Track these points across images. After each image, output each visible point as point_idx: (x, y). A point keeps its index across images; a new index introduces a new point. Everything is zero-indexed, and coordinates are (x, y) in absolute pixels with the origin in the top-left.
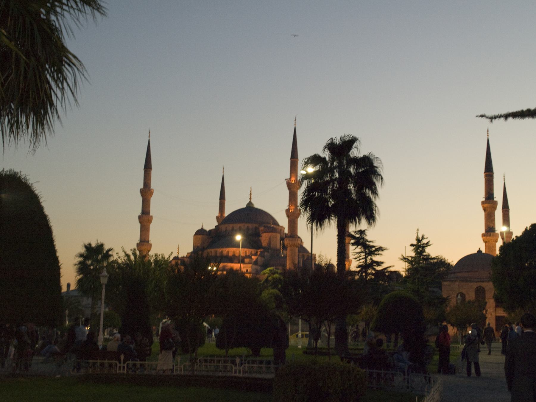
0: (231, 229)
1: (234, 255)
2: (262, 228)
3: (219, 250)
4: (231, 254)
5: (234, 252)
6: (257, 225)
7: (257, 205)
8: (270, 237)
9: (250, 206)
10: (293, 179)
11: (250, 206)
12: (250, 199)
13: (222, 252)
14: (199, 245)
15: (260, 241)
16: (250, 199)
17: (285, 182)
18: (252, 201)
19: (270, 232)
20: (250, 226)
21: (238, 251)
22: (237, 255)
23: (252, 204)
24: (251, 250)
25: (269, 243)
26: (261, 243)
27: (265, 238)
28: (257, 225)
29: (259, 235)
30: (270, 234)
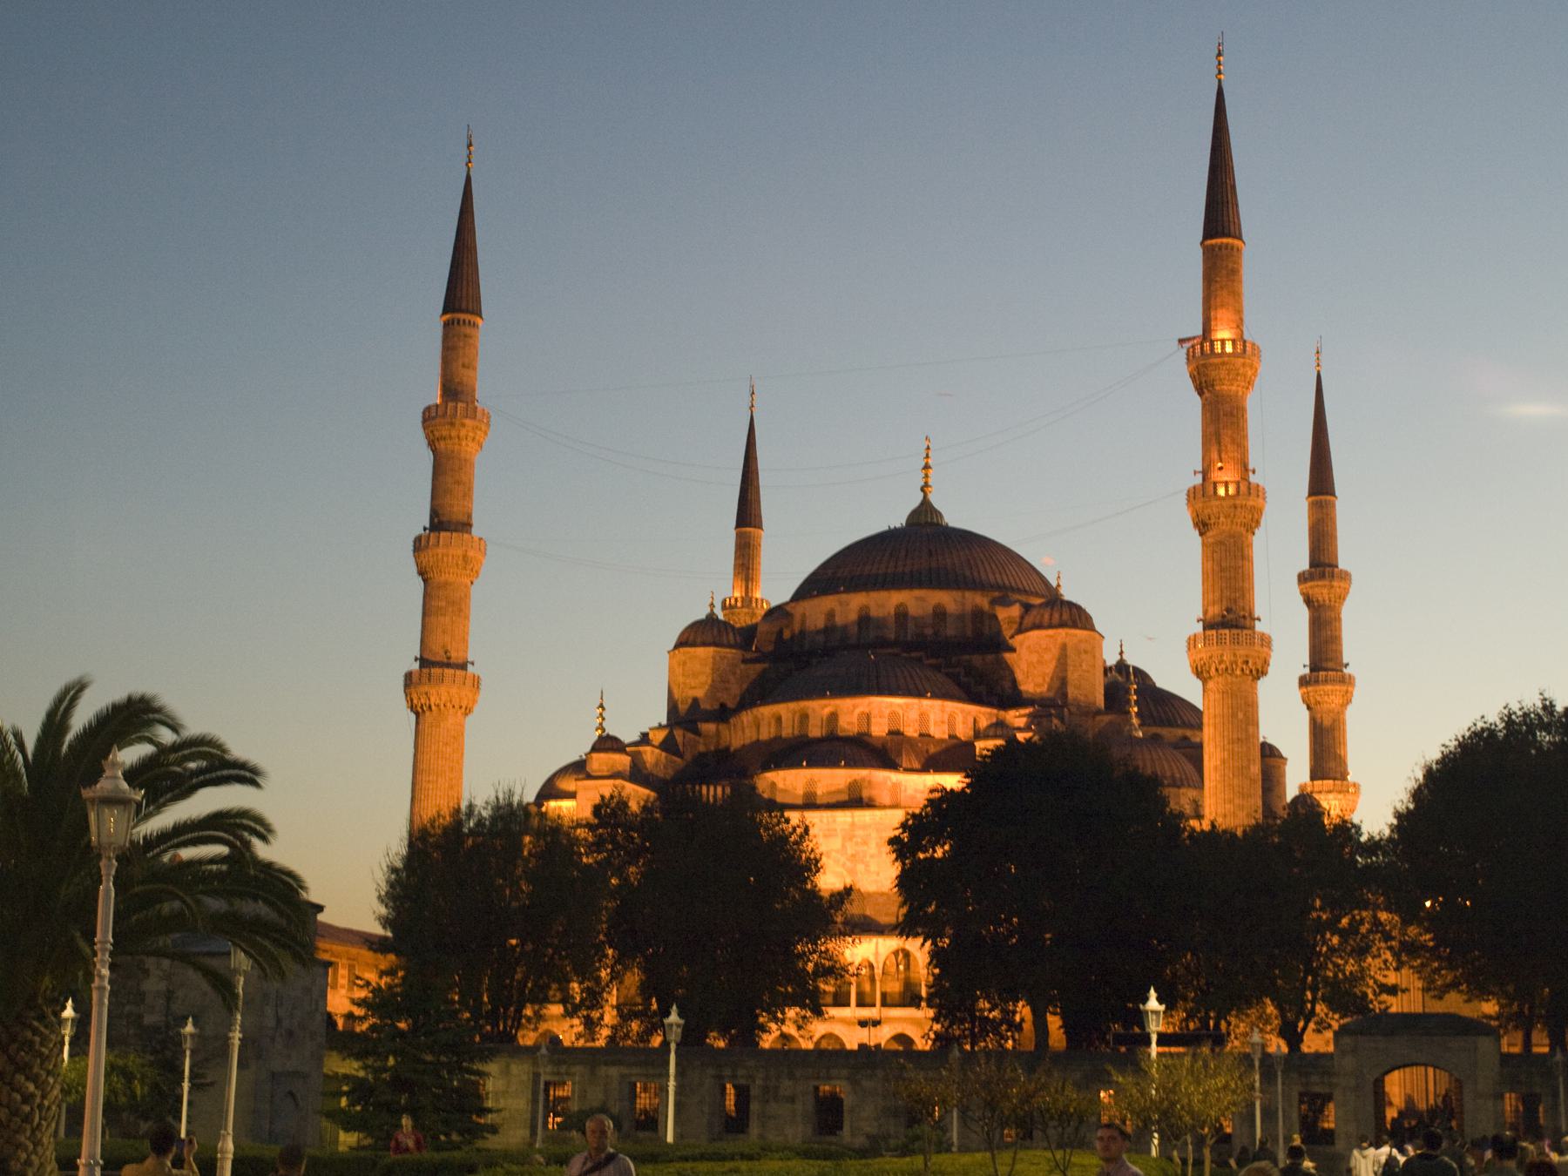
0: (853, 617)
1: (895, 733)
2: (1008, 614)
3: (820, 708)
4: (879, 730)
5: (893, 716)
6: (981, 600)
7: (956, 516)
8: (1064, 647)
9: (925, 519)
10: (1223, 333)
11: (924, 516)
13: (833, 717)
17: (1182, 354)
18: (936, 501)
19: (1062, 625)
20: (947, 599)
21: (913, 715)
22: (911, 731)
23: (938, 514)
25: (1061, 682)
26: (1014, 681)
27: (1033, 659)
28: (981, 600)
29: (998, 645)
30: (1062, 633)
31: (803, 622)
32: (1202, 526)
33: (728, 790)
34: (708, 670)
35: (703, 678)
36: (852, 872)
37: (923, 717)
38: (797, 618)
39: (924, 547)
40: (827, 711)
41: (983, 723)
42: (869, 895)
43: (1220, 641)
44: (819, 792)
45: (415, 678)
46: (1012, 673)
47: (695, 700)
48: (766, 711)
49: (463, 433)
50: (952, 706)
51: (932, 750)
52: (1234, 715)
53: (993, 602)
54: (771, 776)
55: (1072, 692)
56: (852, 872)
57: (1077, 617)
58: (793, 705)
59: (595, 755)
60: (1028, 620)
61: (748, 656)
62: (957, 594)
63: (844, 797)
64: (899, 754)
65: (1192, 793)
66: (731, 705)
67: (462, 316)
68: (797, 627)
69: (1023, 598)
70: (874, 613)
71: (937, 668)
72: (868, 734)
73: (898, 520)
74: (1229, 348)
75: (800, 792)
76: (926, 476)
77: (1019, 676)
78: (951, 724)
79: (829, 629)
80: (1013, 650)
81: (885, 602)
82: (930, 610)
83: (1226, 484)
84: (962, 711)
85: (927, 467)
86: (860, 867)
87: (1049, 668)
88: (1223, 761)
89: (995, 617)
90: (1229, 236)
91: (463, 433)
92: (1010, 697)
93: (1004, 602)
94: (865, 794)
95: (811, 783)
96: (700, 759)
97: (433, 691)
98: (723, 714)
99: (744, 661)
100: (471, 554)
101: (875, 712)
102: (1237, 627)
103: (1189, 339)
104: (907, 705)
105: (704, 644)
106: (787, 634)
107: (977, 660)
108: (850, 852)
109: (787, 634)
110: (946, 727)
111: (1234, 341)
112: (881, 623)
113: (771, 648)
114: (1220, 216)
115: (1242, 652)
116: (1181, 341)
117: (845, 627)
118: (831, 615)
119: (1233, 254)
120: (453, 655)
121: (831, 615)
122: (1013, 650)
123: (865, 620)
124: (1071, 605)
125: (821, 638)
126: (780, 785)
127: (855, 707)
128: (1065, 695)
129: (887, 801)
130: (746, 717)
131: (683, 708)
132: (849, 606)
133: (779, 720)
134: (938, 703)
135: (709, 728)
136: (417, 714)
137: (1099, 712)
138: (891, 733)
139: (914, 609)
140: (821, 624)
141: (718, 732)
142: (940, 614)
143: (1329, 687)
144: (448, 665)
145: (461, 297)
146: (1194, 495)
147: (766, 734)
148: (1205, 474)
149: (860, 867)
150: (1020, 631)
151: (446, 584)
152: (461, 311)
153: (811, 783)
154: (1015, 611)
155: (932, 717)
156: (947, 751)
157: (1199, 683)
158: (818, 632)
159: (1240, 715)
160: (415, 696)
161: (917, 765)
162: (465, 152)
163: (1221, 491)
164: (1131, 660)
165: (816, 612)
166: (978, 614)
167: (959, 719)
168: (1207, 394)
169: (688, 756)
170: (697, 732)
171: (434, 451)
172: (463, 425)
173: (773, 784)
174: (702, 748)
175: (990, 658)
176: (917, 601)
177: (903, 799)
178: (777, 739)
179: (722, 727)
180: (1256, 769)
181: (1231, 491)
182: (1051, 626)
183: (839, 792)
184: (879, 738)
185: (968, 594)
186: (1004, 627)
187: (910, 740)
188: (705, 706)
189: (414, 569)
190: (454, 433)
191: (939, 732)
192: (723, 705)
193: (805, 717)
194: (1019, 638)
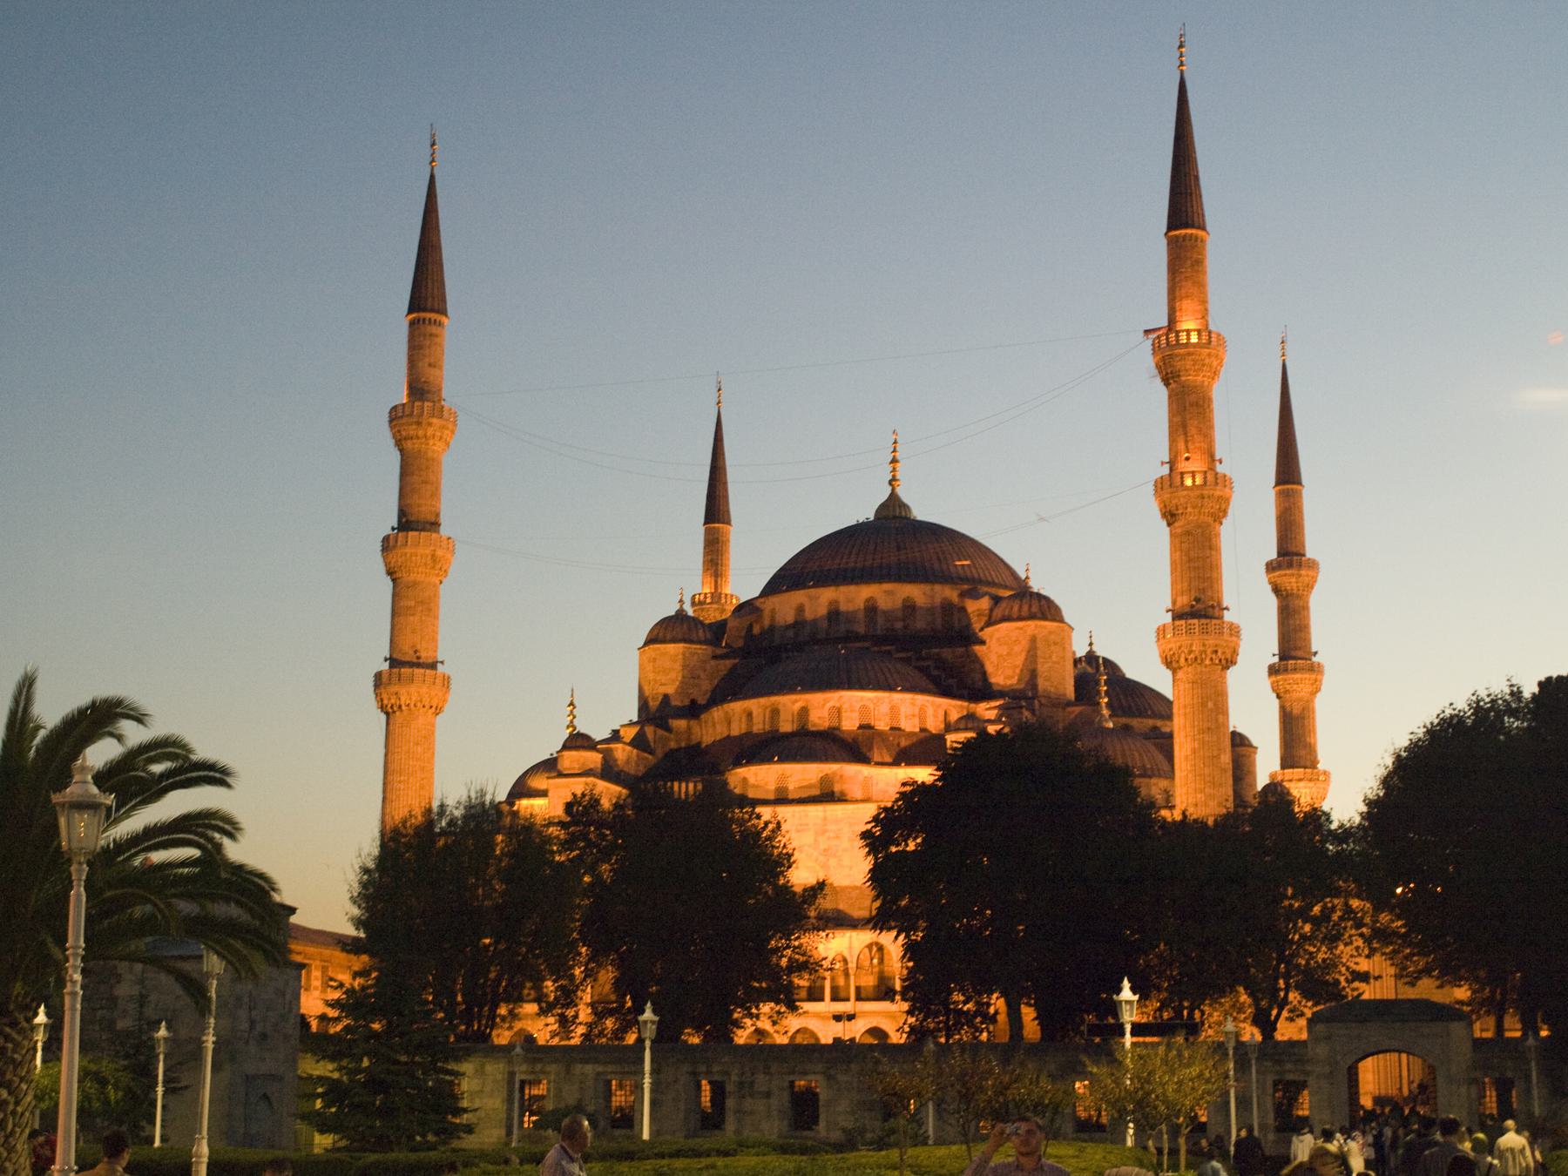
0: (822, 611)
2: (977, 607)
4: (850, 724)
6: (950, 593)
7: (923, 509)
8: (1033, 640)
9: (893, 513)
10: (1188, 324)
11: (893, 513)
12: (893, 481)
13: (804, 712)
14: (670, 690)
15: (978, 662)
16: (893, 481)
18: (904, 495)
19: (1032, 617)
20: (916, 593)
21: (884, 709)
22: (882, 725)
24: (944, 702)
26: (984, 673)
27: (1002, 651)
28: (950, 593)
29: (967, 638)
30: (1031, 626)
31: (773, 618)
32: (1170, 516)
33: (700, 787)
34: (678, 666)
35: (673, 675)
36: (825, 866)
37: (894, 711)
38: (767, 613)
39: (893, 541)
40: (797, 706)
41: (954, 716)
42: (844, 889)
43: (1189, 632)
44: (791, 787)
45: (385, 678)
46: (982, 666)
47: (666, 697)
48: (737, 707)
49: (430, 432)
50: (921, 699)
51: (904, 743)
52: (1204, 705)
53: (962, 595)
54: (740, 771)
55: (1042, 684)
56: (825, 866)
57: (1045, 609)
58: (763, 701)
59: (566, 753)
60: (998, 613)
61: (719, 652)
62: (927, 588)
63: (816, 792)
64: (871, 748)
65: (1163, 783)
66: (702, 701)
67: (428, 315)
68: (767, 623)
69: (993, 591)
70: (843, 607)
71: (907, 661)
72: (838, 729)
73: (867, 512)
74: (1194, 339)
75: (772, 787)
76: (894, 470)
77: (989, 668)
78: (922, 718)
79: (799, 624)
80: (983, 642)
81: (854, 597)
82: (899, 604)
83: (1193, 474)
84: (933, 704)
85: (894, 461)
86: (833, 862)
87: (1019, 660)
88: (1194, 751)
89: (963, 609)
90: (1193, 227)
91: (430, 432)
92: (980, 690)
93: (974, 594)
94: (837, 788)
95: (783, 777)
96: (671, 755)
97: (403, 691)
98: (694, 710)
99: (715, 657)
100: (439, 553)
101: (845, 706)
102: (1206, 617)
103: (1154, 330)
104: (878, 699)
105: (674, 641)
106: (756, 630)
107: (947, 653)
108: (822, 847)
109: (756, 630)
110: (916, 721)
111: (1199, 331)
112: (850, 617)
113: (740, 643)
114: (1184, 208)
115: (1211, 641)
116: (1147, 332)
117: (815, 621)
118: (800, 609)
119: (1197, 245)
120: (423, 654)
121: (800, 609)
122: (983, 642)
123: (834, 614)
124: (1039, 596)
125: (791, 633)
126: (752, 781)
127: (826, 701)
128: (1034, 686)
129: (859, 796)
130: (717, 713)
131: (654, 704)
132: (818, 601)
133: (750, 715)
134: (908, 696)
135: (680, 724)
136: (387, 714)
137: (1069, 704)
138: (861, 727)
139: (884, 603)
140: (790, 619)
141: (689, 728)
142: (909, 607)
143: (1298, 676)
144: (419, 665)
145: (426, 296)
146: (1160, 485)
147: (735, 732)
148: (1172, 464)
149: (833, 862)
150: (989, 623)
151: (415, 584)
152: (425, 310)
153: (783, 777)
154: (985, 603)
155: (903, 710)
156: (921, 742)
157: (1169, 673)
158: (788, 627)
159: (1210, 705)
160: (385, 696)
161: (888, 759)
162: (428, 151)
163: (1188, 482)
164: (1100, 652)
165: (785, 608)
166: (948, 608)
167: (930, 711)
168: (1173, 385)
169: (660, 753)
170: (669, 729)
171: (401, 451)
172: (430, 424)
173: (745, 779)
174: (673, 745)
175: (961, 650)
176: (888, 595)
177: (875, 794)
178: (748, 734)
179: (692, 722)
180: (1226, 758)
181: (1198, 481)
182: (1020, 619)
183: (810, 786)
184: (850, 732)
185: (938, 588)
186: (974, 619)
187: (880, 734)
188: (675, 702)
189: (383, 569)
190: (421, 433)
191: (910, 725)
192: (693, 702)
193: (775, 712)
194: (988, 630)
